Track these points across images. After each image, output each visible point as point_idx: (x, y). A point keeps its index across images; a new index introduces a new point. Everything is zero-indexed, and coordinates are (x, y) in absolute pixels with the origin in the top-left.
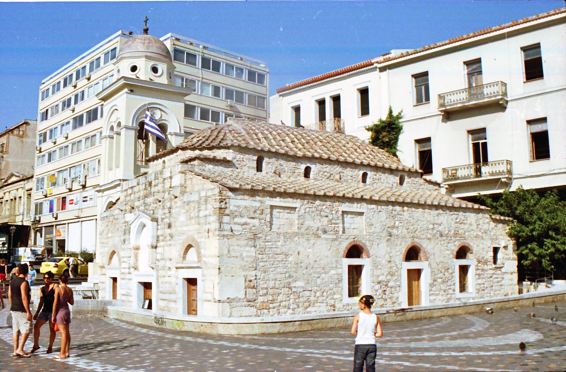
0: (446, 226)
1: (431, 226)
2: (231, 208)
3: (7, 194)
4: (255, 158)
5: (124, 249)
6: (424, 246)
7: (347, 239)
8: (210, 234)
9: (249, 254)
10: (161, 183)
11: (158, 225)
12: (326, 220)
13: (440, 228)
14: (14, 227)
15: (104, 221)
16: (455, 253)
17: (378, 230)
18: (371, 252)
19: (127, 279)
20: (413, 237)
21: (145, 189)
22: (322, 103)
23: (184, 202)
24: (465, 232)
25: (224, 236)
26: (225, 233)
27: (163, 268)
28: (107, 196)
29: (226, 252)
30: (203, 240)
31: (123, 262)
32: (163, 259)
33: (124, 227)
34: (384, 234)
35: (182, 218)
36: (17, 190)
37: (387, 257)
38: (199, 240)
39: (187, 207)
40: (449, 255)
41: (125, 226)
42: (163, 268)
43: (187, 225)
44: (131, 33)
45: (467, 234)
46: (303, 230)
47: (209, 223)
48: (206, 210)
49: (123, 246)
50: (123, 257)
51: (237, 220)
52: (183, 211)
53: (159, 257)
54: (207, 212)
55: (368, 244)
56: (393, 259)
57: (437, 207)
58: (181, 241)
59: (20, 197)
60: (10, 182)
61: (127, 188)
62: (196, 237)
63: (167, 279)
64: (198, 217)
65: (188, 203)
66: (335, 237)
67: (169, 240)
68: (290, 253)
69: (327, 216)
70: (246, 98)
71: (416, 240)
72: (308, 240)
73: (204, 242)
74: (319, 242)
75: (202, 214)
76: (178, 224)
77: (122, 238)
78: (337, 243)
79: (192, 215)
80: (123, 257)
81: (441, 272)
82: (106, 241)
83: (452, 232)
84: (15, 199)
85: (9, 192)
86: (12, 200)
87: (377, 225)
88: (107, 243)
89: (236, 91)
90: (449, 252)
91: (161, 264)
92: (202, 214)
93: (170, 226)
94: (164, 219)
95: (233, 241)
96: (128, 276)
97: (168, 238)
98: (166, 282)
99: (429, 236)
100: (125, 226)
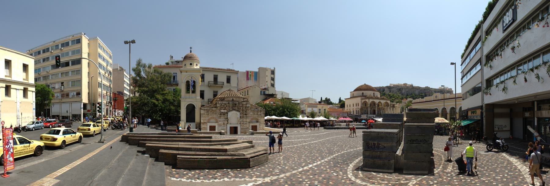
5: (220, 119)
11: (240, 114)
27: (243, 123)
28: (187, 102)
35: (251, 113)
42: (243, 123)
49: (219, 118)
52: (251, 112)
53: (241, 121)
61: (221, 103)
63: (245, 126)
65: (254, 111)
75: (259, 113)
77: (219, 116)
79: (255, 113)
96: (223, 125)
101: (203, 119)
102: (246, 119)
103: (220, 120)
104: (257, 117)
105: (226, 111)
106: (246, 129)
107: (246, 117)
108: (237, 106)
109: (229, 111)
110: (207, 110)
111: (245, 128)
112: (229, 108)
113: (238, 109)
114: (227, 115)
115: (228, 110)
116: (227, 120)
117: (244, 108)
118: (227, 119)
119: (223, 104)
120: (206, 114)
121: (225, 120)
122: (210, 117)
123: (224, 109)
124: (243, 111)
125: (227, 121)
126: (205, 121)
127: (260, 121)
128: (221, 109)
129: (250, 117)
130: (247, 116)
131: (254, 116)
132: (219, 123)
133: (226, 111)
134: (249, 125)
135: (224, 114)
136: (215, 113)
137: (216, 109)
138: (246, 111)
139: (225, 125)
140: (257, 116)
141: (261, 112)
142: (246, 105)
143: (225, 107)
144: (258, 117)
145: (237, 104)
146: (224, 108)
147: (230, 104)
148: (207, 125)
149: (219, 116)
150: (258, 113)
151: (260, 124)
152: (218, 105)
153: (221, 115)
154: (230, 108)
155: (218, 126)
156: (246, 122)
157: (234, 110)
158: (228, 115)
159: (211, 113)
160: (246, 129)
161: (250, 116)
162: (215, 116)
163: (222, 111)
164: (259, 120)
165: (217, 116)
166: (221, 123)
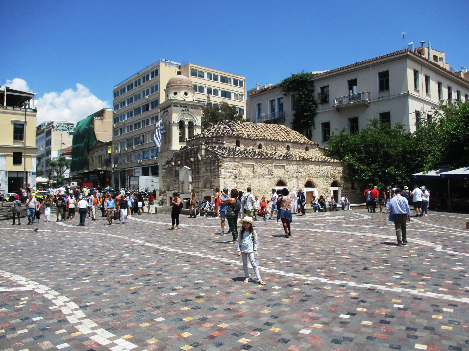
0: (326, 171)
1: (318, 171)
2: (225, 165)
3: (96, 153)
4: (236, 141)
5: (175, 184)
6: (315, 181)
7: (277, 178)
8: (216, 177)
9: (233, 185)
11: (192, 172)
12: (267, 169)
13: (323, 172)
14: (103, 172)
16: (331, 184)
17: (291, 174)
18: (289, 184)
20: (309, 177)
21: (185, 156)
22: (272, 102)
24: (336, 174)
25: (222, 177)
26: (223, 176)
29: (223, 184)
30: (213, 179)
31: (176, 189)
34: (294, 175)
35: (204, 169)
36: (102, 150)
37: (296, 186)
38: (211, 179)
40: (327, 185)
44: (166, 61)
45: (337, 175)
46: (256, 174)
48: (214, 166)
49: (175, 182)
51: (227, 170)
55: (287, 180)
56: (299, 187)
57: (322, 162)
59: (104, 155)
60: (97, 146)
62: (210, 177)
64: (211, 169)
66: (271, 177)
68: (251, 184)
69: (267, 168)
70: (232, 95)
71: (310, 178)
72: (259, 179)
74: (264, 179)
75: (212, 168)
76: (201, 172)
78: (272, 180)
79: (208, 169)
81: (323, 193)
82: (165, 180)
83: (329, 174)
84: (101, 156)
85: (97, 151)
86: (99, 156)
87: (291, 171)
89: (227, 92)
90: (327, 184)
92: (212, 168)
93: (198, 173)
95: (226, 180)
97: (197, 178)
99: (317, 176)
102: (198, 182)
119: (177, 157)
124: (194, 165)
130: (200, 175)
138: (198, 165)
140: (210, 174)
148: (166, 196)
149: (174, 178)
150: (211, 167)
161: (202, 175)
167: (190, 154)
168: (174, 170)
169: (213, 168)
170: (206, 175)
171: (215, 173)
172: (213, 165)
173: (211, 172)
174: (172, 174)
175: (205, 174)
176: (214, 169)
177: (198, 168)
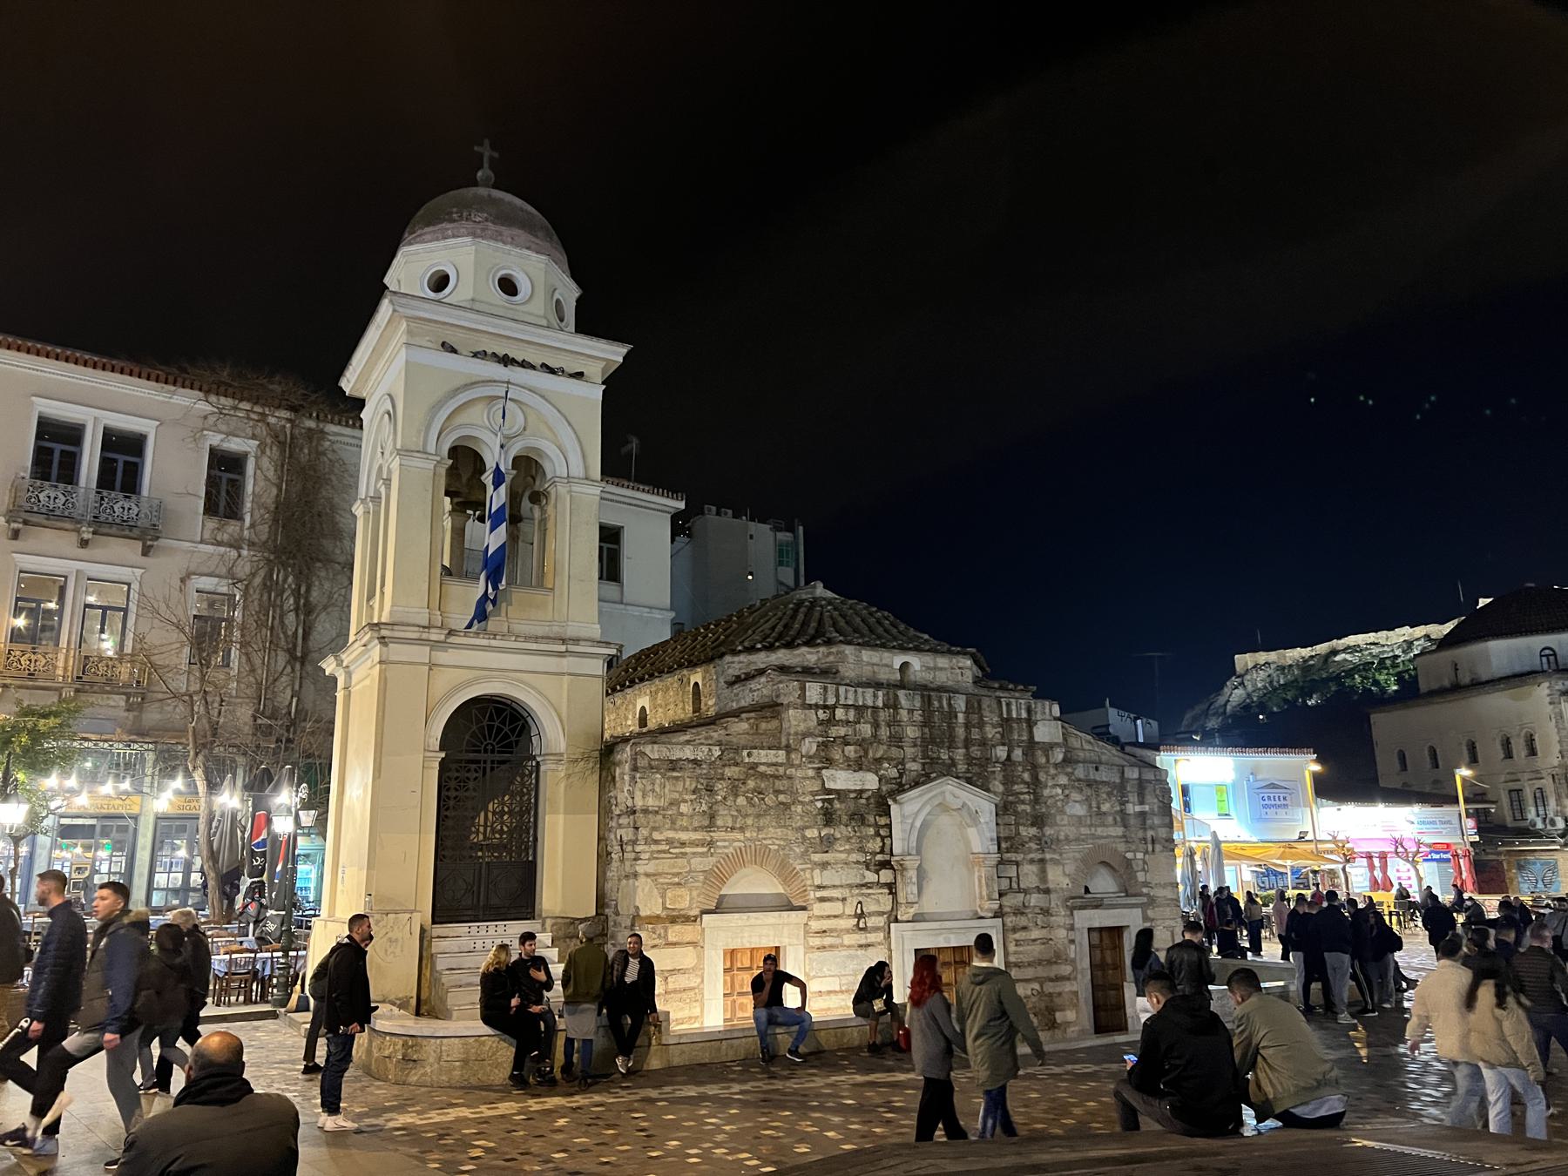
5: (824, 865)
8: (1158, 847)
10: (994, 726)
15: (675, 774)
19: (849, 947)
23: (1079, 780)
27: (1019, 912)
30: (1140, 855)
31: (822, 900)
32: (1020, 890)
33: (819, 804)
35: (1079, 810)
38: (1129, 855)
39: (1088, 792)
41: (824, 801)
42: (1019, 912)
43: (1091, 825)
47: (1152, 828)
48: (1142, 803)
49: (817, 857)
50: (820, 887)
52: (1075, 796)
54: (1147, 808)
58: (1077, 855)
61: (831, 701)
63: (1035, 934)
64: (1122, 812)
67: (1038, 849)
73: (1145, 862)
77: (812, 833)
79: (1105, 807)
80: (820, 887)
88: (711, 844)
91: (1011, 901)
92: (1132, 808)
93: (1039, 821)
94: (1012, 803)
96: (849, 939)
97: (1033, 845)
98: (1034, 940)
100: (830, 801)
101: (647, 875)
103: (828, 877)
104: (1121, 847)
105: (870, 781)
106: (1050, 963)
107: (1043, 843)
108: (960, 732)
109: (901, 789)
110: (695, 762)
111: (1039, 962)
112: (895, 752)
113: (969, 760)
114: (883, 821)
115: (893, 773)
116: (886, 876)
117: (1018, 754)
118: (886, 865)
119: (840, 714)
120: (684, 808)
121: (871, 877)
122: (729, 842)
123: (858, 765)
125: (891, 888)
126: (684, 900)
127: (1146, 884)
128: (829, 762)
129: (1068, 840)
130: (1048, 831)
131: (1100, 832)
132: (818, 909)
133: (870, 781)
134: (1072, 928)
135: (858, 818)
136: (770, 800)
137: (781, 756)
139: (872, 937)
140: (1119, 831)
141: (1149, 798)
142: (1031, 723)
143: (862, 744)
144: (1126, 839)
145: (961, 716)
146: (850, 750)
147: (904, 714)
150: (1123, 803)
151: (1150, 913)
152: (795, 720)
153: (828, 817)
154: (910, 751)
155: (809, 949)
156: (1035, 900)
157: (948, 770)
158: (889, 826)
159: (741, 801)
160: (1050, 963)
161: (1071, 832)
162: (773, 835)
163: (841, 779)
164: (1141, 877)
165: (791, 835)
166: (836, 908)
167: (968, 726)
168: (816, 787)
169: (1138, 808)
170: (1093, 836)
171: (1150, 833)
172: (1133, 797)
173: (1125, 826)
174: (786, 806)
175: (1084, 830)
176: (1143, 814)
177: (1037, 800)
